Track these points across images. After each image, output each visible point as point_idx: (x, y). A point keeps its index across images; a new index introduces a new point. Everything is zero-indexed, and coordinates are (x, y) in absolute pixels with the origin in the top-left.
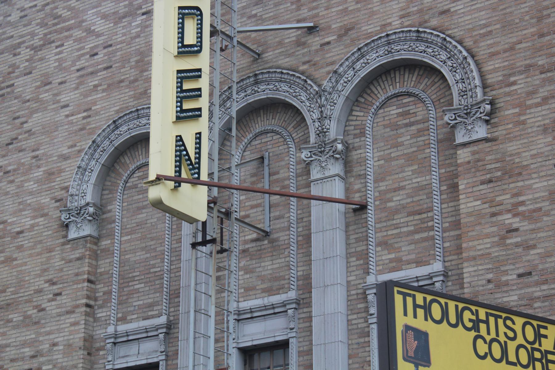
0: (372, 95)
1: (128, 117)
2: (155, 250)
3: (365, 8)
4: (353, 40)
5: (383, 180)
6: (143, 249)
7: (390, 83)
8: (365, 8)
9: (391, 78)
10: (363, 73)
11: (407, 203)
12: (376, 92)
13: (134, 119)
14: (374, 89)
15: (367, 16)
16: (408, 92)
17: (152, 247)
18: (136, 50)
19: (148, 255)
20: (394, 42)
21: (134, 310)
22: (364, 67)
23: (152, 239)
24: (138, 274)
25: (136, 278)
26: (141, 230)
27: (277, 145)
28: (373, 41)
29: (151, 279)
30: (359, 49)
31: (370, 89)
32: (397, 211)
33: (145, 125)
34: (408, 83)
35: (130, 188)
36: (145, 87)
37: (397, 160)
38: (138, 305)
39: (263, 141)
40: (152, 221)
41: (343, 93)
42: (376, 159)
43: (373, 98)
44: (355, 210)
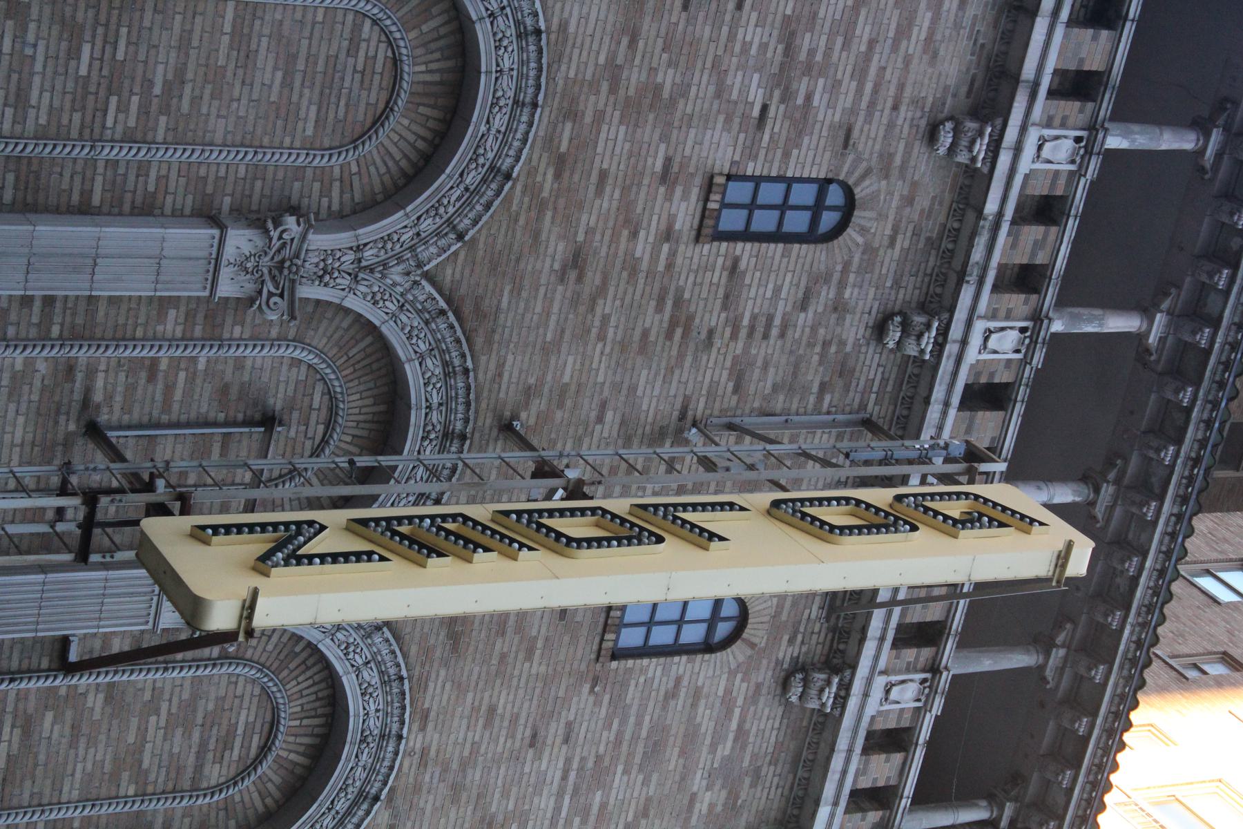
0: (303, 667)
1: (532, 73)
2: (165, 109)
3: (483, 674)
4: (427, 652)
5: (109, 699)
6: (180, 73)
7: (306, 707)
8: (483, 674)
9: (315, 709)
10: (349, 683)
11: (36, 755)
12: (300, 679)
13: (518, 89)
14: (309, 674)
15: (465, 678)
16: (270, 749)
17: (175, 101)
18: (689, 86)
19: (157, 90)
20: (380, 747)
21: (24, 43)
22: (360, 685)
23: (196, 100)
24: (120, 56)
25: (108, 49)
26: (231, 66)
27: (289, 449)
28: (403, 708)
29: (91, 97)
30: (401, 679)
31: (314, 665)
32: (27, 733)
33: (488, 122)
34: (289, 747)
35: (357, 28)
36: (583, 114)
37: (139, 728)
38: (33, 58)
39: (314, 415)
40: (244, 101)
41: (328, 641)
42: (159, 685)
43: (292, 671)
44: (65, 642)
